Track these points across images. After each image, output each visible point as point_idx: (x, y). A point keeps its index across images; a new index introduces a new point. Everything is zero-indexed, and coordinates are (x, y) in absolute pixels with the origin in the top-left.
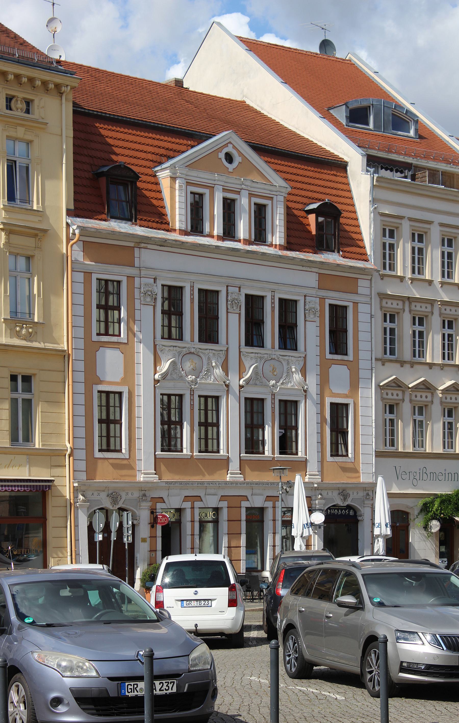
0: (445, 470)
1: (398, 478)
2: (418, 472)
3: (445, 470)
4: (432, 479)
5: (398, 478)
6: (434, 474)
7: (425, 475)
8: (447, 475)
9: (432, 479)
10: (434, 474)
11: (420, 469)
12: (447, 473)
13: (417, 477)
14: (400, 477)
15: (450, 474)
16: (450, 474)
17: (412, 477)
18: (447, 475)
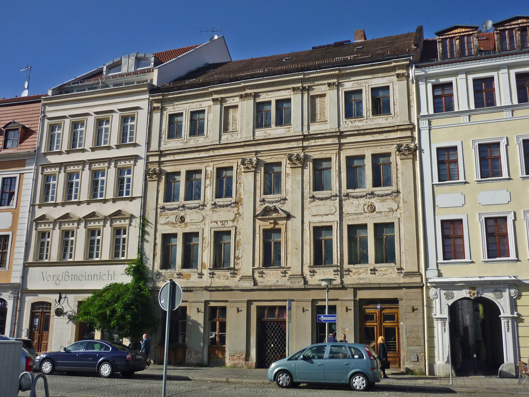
0: (86, 273)
1: (44, 280)
2: (61, 275)
3: (86, 273)
4: (73, 279)
5: (44, 280)
6: (76, 276)
7: (67, 277)
8: (87, 277)
9: (73, 279)
10: (76, 276)
11: (63, 273)
12: (87, 275)
13: (60, 279)
14: (45, 279)
15: (90, 276)
16: (90, 276)
17: (55, 278)
18: (87, 277)
